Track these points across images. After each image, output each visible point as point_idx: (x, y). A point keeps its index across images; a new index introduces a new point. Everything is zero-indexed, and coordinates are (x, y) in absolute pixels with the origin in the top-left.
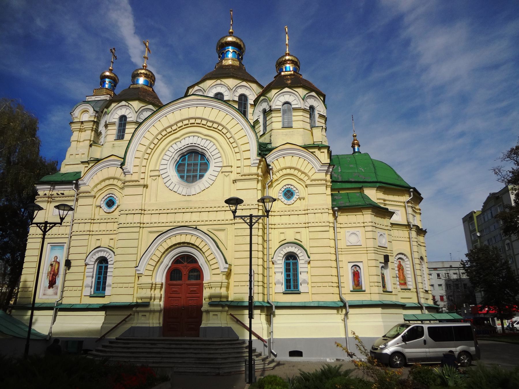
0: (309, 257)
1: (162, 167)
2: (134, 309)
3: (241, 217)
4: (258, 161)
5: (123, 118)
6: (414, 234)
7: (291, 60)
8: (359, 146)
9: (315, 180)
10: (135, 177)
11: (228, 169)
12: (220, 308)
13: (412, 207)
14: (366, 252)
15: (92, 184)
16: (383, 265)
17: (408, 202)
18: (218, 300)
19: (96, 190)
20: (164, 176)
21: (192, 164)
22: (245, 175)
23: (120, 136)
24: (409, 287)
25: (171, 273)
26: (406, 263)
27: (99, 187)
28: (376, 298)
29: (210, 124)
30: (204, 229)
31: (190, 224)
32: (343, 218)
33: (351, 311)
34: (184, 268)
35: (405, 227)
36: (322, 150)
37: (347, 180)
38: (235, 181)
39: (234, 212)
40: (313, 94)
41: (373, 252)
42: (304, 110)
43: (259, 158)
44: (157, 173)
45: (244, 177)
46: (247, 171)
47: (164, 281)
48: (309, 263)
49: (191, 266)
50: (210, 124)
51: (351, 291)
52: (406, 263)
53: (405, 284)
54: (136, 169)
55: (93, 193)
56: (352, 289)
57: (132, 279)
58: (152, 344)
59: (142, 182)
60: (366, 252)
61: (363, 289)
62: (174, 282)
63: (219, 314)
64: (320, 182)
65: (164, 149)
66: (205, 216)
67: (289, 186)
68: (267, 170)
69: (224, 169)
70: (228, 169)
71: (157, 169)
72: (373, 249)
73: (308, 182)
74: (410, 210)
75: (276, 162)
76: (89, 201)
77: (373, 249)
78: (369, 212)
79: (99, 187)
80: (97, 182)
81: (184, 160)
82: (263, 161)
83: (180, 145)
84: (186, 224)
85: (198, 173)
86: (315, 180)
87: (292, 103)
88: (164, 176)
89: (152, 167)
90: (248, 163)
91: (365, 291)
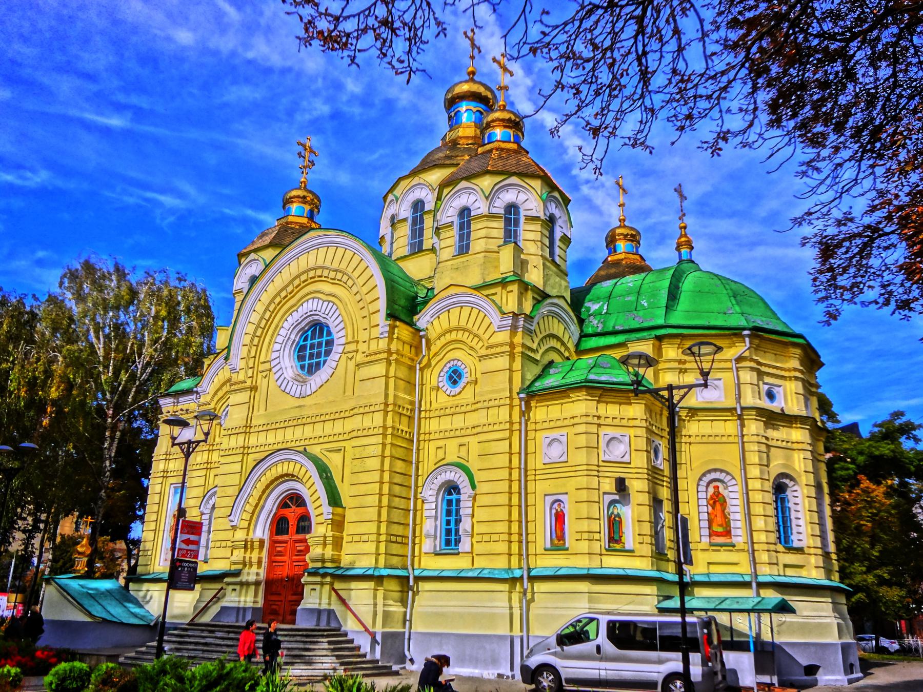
0: (474, 487)
2: (226, 580)
3: (179, 444)
4: (387, 329)
6: (754, 427)
7: (503, 120)
8: (692, 248)
9: (491, 347)
10: (241, 377)
11: (352, 347)
12: (318, 579)
13: (752, 369)
14: (596, 473)
15: (212, 389)
16: (617, 497)
17: (740, 359)
18: (319, 565)
19: (216, 399)
21: (314, 345)
22: (370, 355)
24: (734, 540)
25: (278, 524)
26: (730, 489)
27: (220, 394)
28: (581, 564)
29: (332, 275)
30: (316, 450)
31: (293, 444)
32: (540, 412)
33: (540, 587)
34: (292, 514)
35: (729, 414)
36: (509, 288)
37: (611, 329)
39: (174, 438)
40: (514, 180)
41: (585, 473)
43: (388, 322)
44: (267, 366)
45: (369, 359)
46: (374, 347)
47: (266, 537)
48: (474, 499)
49: (300, 510)
50: (332, 275)
51: (546, 550)
52: (730, 489)
53: (728, 533)
56: (548, 546)
57: (228, 535)
58: (211, 632)
60: (596, 473)
61: (567, 545)
62: (280, 538)
63: (318, 587)
64: (499, 350)
65: (277, 326)
66: (318, 430)
67: (455, 362)
68: (419, 338)
70: (352, 347)
72: (585, 467)
73: (483, 352)
74: (747, 377)
77: (585, 467)
78: (583, 394)
79: (220, 394)
81: (306, 339)
82: (397, 326)
83: (296, 316)
84: (284, 446)
85: (322, 359)
86: (491, 347)
88: (274, 370)
89: (262, 359)
90: (376, 332)
91: (567, 549)
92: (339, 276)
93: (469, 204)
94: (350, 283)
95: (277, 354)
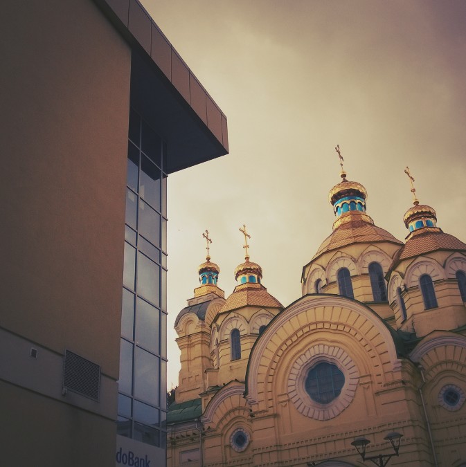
1: (291, 389)
4: (400, 365)
5: (235, 333)
10: (262, 407)
11: (367, 380)
15: (216, 420)
19: (221, 426)
20: (294, 400)
23: (236, 355)
27: (225, 422)
38: (377, 393)
39: (363, 454)
42: (450, 280)
43: (400, 360)
46: (390, 378)
50: (334, 327)
54: (261, 397)
55: (219, 431)
59: (271, 411)
65: (288, 367)
69: (362, 381)
71: (285, 392)
75: (425, 358)
76: (217, 441)
80: (221, 416)
83: (304, 359)
87: (431, 275)
88: (294, 400)
90: (390, 367)
92: (341, 327)
93: (428, 273)
94: (353, 332)
95: (293, 388)
